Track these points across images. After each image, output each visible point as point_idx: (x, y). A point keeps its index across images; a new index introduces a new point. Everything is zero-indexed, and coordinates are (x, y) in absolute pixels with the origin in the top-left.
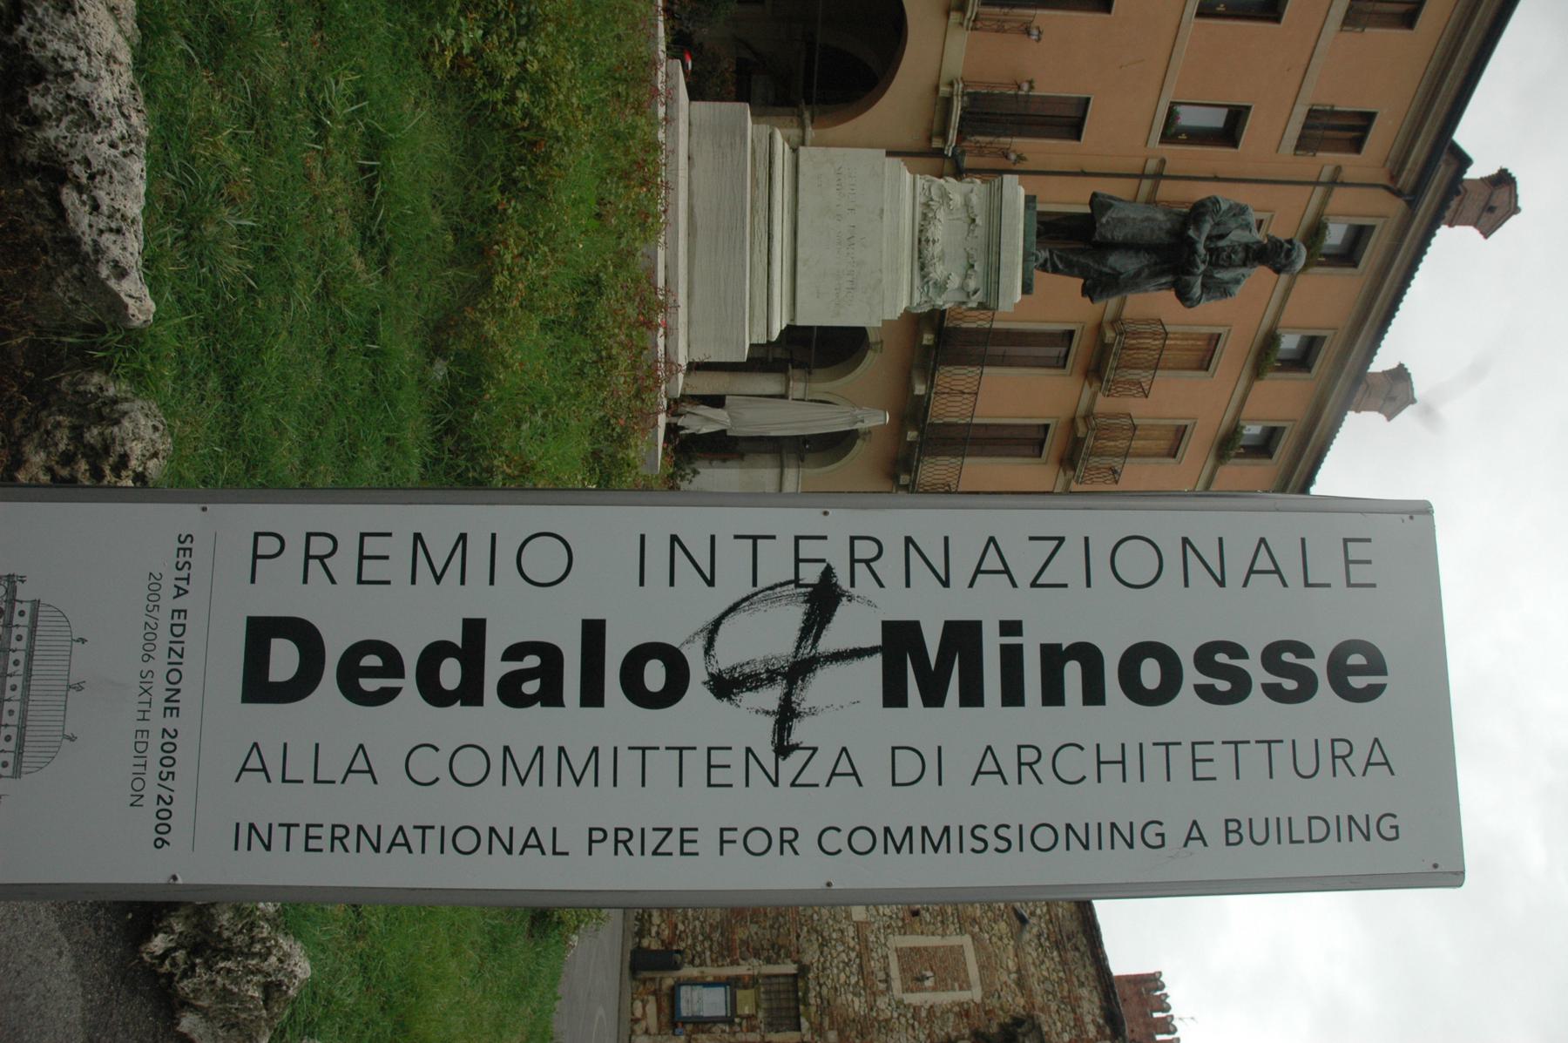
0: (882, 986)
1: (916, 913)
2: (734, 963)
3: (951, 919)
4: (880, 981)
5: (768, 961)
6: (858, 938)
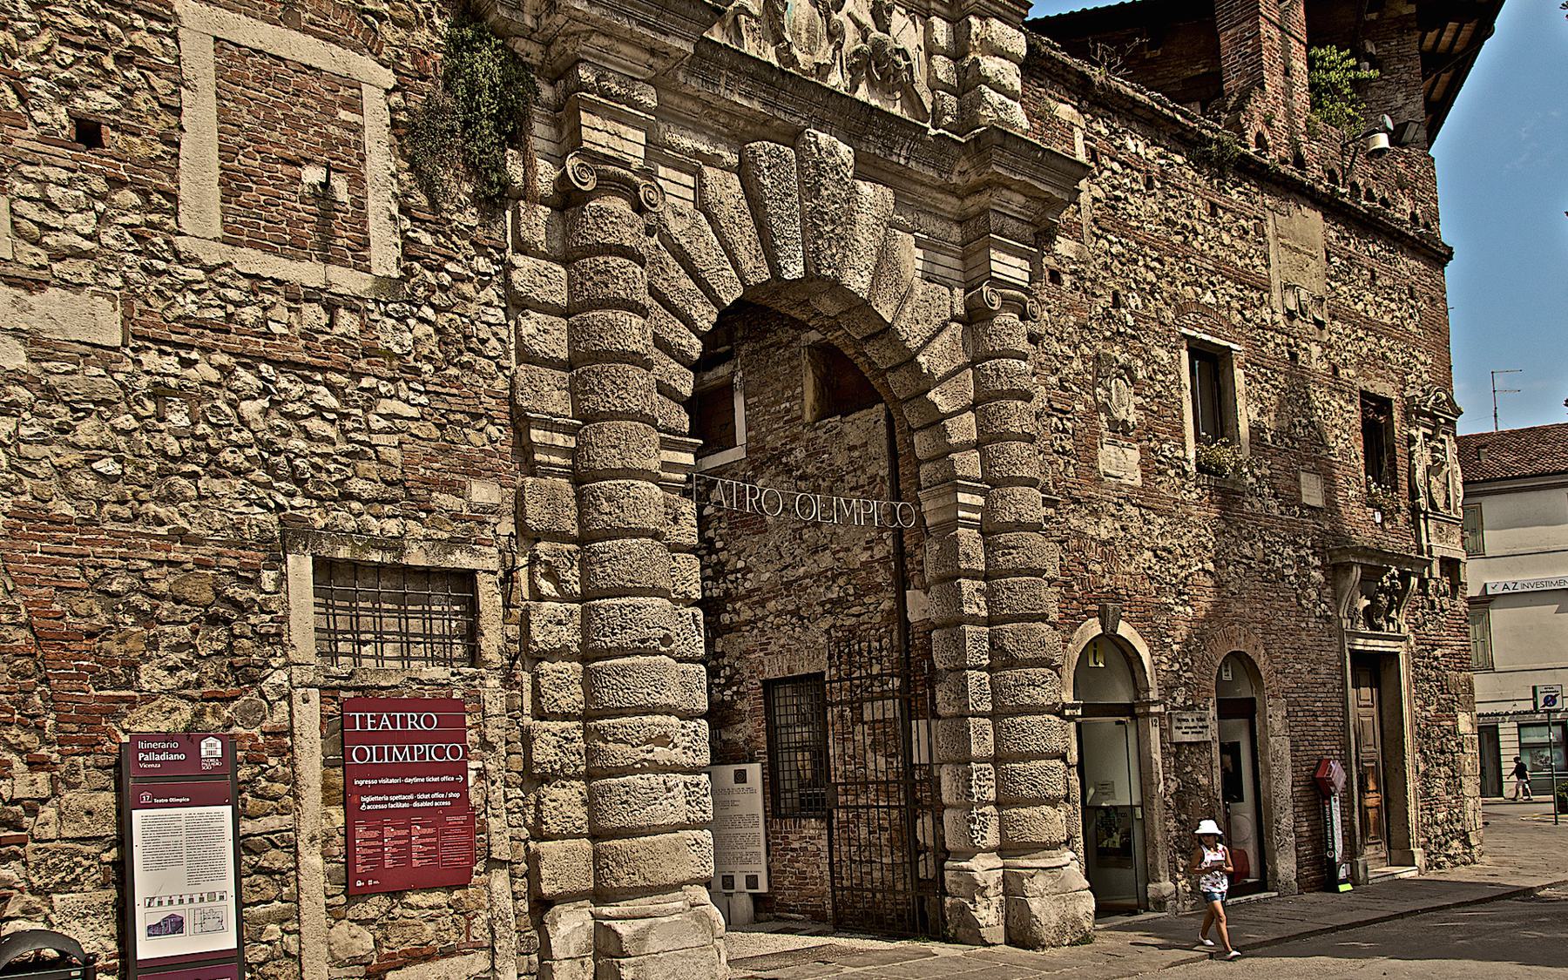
0: (347, 323)
1: (88, 132)
2: (282, 741)
3: (112, 28)
4: (331, 325)
5: (275, 638)
6: (191, 347)
